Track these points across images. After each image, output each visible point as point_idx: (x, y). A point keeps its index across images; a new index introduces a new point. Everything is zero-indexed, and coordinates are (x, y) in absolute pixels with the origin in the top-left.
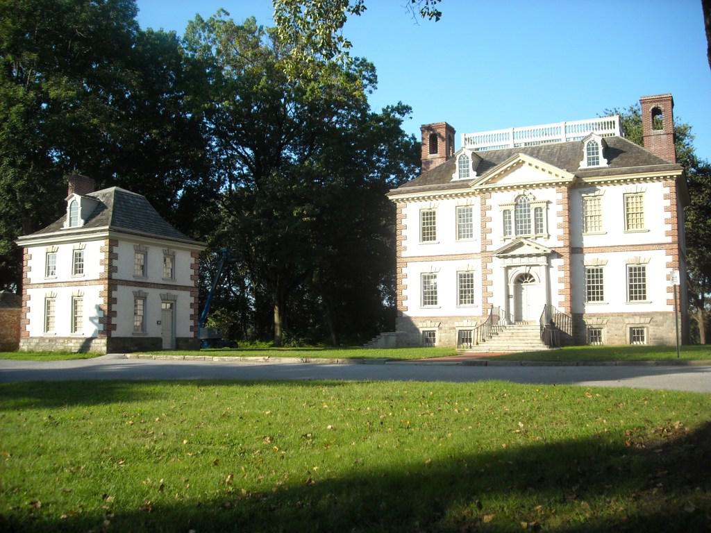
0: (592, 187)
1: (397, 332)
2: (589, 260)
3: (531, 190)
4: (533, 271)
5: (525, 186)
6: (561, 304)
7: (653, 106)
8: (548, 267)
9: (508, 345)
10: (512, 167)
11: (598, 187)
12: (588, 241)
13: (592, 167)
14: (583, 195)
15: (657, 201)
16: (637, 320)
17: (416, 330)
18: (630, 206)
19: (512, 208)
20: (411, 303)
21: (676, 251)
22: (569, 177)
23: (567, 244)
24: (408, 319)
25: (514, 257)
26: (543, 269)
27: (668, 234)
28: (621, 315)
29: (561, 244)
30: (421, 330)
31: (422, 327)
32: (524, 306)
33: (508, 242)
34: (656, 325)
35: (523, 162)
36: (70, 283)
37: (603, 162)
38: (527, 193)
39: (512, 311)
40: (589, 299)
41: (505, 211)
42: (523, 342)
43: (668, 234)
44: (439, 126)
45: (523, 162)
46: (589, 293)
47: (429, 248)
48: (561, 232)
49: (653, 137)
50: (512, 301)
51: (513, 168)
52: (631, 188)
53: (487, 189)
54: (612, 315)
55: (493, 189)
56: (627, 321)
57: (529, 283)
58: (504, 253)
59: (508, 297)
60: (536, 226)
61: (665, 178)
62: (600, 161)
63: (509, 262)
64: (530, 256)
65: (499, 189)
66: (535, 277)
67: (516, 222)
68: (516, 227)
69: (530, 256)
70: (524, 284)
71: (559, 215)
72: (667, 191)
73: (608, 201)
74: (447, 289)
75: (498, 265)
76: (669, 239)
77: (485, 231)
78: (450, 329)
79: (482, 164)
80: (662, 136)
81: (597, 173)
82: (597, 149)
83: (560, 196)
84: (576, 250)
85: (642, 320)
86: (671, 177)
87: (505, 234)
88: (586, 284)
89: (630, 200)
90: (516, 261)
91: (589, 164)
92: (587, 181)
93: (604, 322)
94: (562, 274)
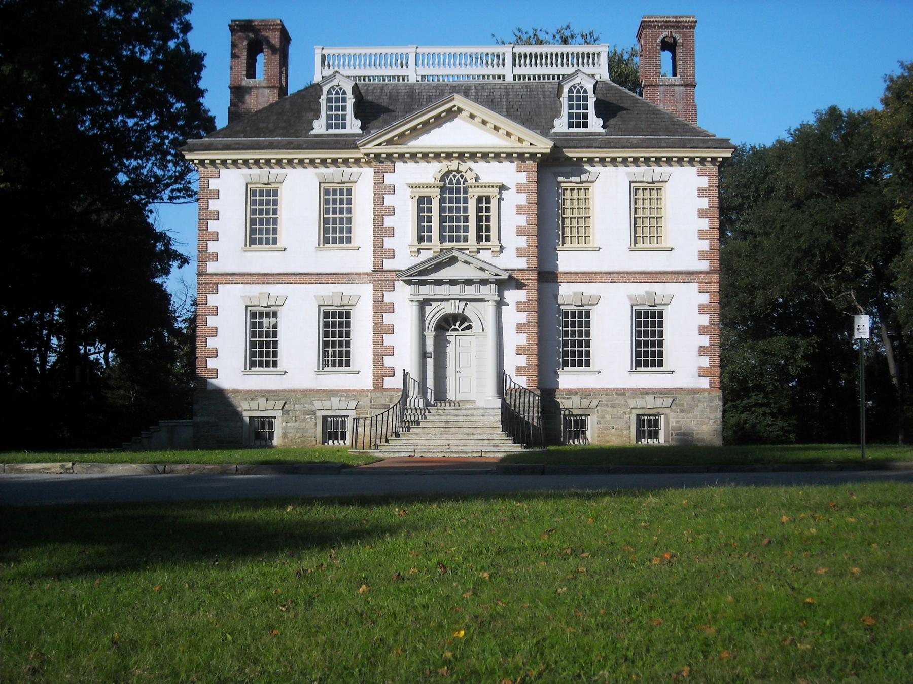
0: (576, 167)
1: (197, 419)
2: (567, 292)
3: (470, 164)
4: (471, 311)
5: (461, 156)
6: (520, 371)
7: (664, 34)
8: (500, 304)
9: (448, 442)
10: (437, 117)
11: (587, 167)
12: (568, 260)
13: (574, 130)
14: (560, 179)
15: (687, 195)
16: (650, 402)
17: (238, 415)
18: (640, 204)
19: (435, 193)
20: (226, 364)
21: (716, 287)
22: (544, 146)
23: (535, 264)
24: (220, 393)
25: (438, 282)
26: (490, 308)
27: (702, 256)
28: (621, 392)
29: (522, 263)
30: (246, 415)
31: (248, 410)
32: (450, 372)
33: (426, 255)
34: (682, 411)
35: (460, 110)
37: (595, 124)
38: (463, 167)
39: (430, 383)
40: (565, 364)
41: (421, 200)
42: (471, 437)
43: (702, 256)
44: (267, 25)
45: (460, 110)
46: (566, 354)
47: (263, 260)
48: (523, 242)
49: (662, 88)
50: (430, 362)
51: (439, 121)
52: (641, 172)
53: (389, 156)
54: (607, 391)
55: (401, 156)
56: (632, 403)
57: (460, 333)
58: (419, 276)
59: (424, 355)
60: (479, 229)
61: (703, 160)
62: (590, 120)
63: (426, 292)
64: (468, 282)
65: (413, 156)
66: (476, 324)
67: (442, 220)
68: (442, 229)
69: (468, 282)
70: (450, 333)
71: (520, 210)
72: (704, 182)
73: (607, 190)
74: (299, 339)
75: (403, 297)
76: (705, 266)
77: (381, 232)
78: (305, 413)
79: (374, 107)
80: (676, 88)
81: (589, 141)
82: (586, 99)
83: (523, 178)
84: (547, 276)
85: (659, 403)
86: (714, 159)
87: (421, 239)
88: (562, 337)
89: (640, 194)
91: (570, 125)
92: (570, 155)
93: (594, 404)
94: (523, 317)
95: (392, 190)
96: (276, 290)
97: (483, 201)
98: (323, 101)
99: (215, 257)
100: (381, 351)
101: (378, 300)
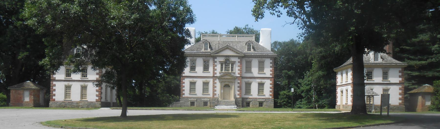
6: (238, 95)
27: (271, 75)
36: (64, 81)
63: (222, 80)
76: (271, 76)
85: (262, 100)
90: (224, 80)
95: (216, 62)
100: (214, 91)
101: (214, 82)
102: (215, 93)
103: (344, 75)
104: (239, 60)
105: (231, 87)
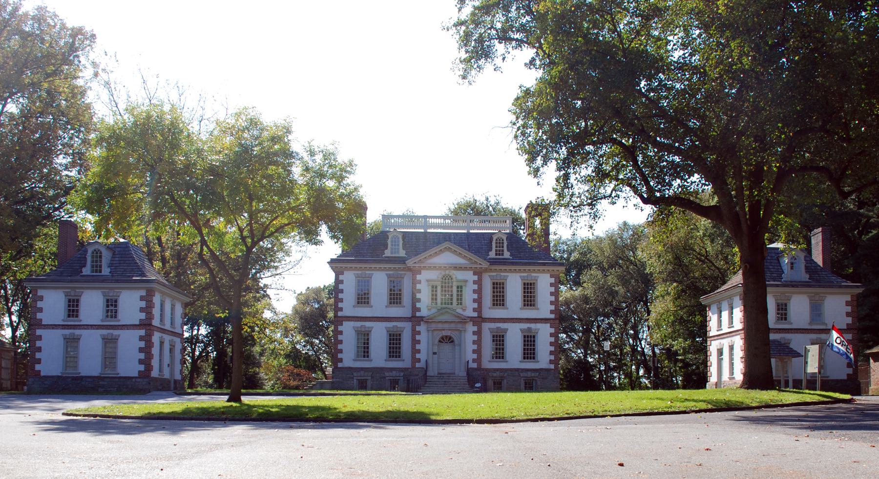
16: (529, 374)
28: (517, 370)
36: (64, 327)
41: (433, 287)
76: (553, 316)
85: (533, 375)
90: (440, 326)
95: (420, 282)
96: (368, 324)
97: (460, 288)
98: (389, 242)
99: (341, 309)
100: (415, 351)
102: (418, 356)
103: (725, 314)
104: (476, 278)
105: (456, 342)
